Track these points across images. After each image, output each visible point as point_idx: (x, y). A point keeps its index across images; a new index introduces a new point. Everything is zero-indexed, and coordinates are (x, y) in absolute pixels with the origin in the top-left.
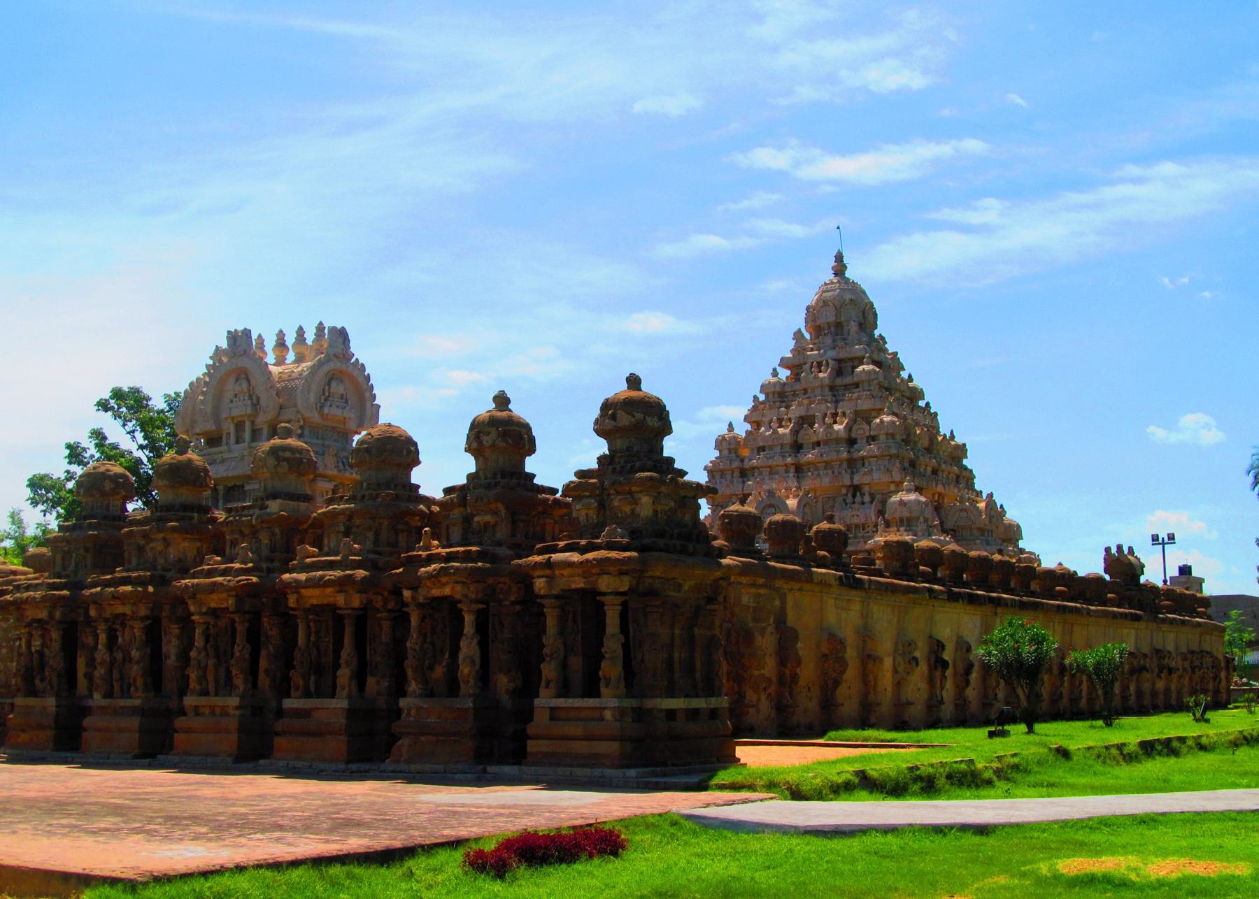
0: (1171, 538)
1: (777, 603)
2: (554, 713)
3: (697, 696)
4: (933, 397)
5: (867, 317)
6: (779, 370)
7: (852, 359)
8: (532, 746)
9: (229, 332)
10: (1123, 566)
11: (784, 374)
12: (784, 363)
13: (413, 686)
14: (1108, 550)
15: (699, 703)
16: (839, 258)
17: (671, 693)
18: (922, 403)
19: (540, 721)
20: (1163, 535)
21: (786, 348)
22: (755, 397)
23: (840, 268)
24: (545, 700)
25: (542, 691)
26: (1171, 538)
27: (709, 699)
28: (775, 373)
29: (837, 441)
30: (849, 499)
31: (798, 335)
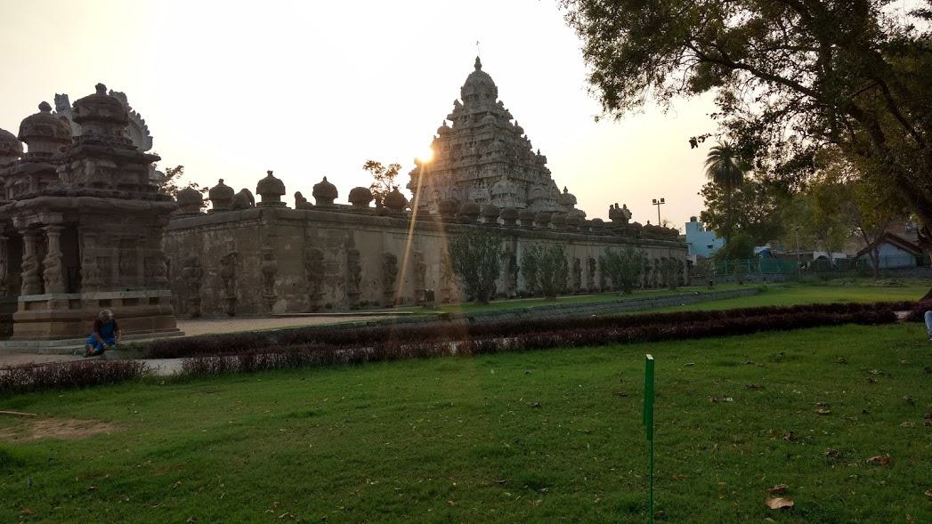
0: (663, 200)
1: (347, 236)
2: (28, 305)
3: (140, 290)
4: (530, 133)
7: (482, 113)
8: (17, 327)
9: (56, 95)
10: (620, 214)
12: (449, 118)
14: (612, 206)
15: (142, 294)
16: (478, 60)
17: (108, 286)
18: (523, 136)
19: (20, 313)
20: (658, 200)
21: (450, 109)
22: (435, 137)
23: (478, 65)
24: (24, 298)
25: (23, 292)
26: (663, 200)
27: (148, 292)
28: (444, 123)
29: (472, 156)
30: (477, 185)
31: (456, 103)
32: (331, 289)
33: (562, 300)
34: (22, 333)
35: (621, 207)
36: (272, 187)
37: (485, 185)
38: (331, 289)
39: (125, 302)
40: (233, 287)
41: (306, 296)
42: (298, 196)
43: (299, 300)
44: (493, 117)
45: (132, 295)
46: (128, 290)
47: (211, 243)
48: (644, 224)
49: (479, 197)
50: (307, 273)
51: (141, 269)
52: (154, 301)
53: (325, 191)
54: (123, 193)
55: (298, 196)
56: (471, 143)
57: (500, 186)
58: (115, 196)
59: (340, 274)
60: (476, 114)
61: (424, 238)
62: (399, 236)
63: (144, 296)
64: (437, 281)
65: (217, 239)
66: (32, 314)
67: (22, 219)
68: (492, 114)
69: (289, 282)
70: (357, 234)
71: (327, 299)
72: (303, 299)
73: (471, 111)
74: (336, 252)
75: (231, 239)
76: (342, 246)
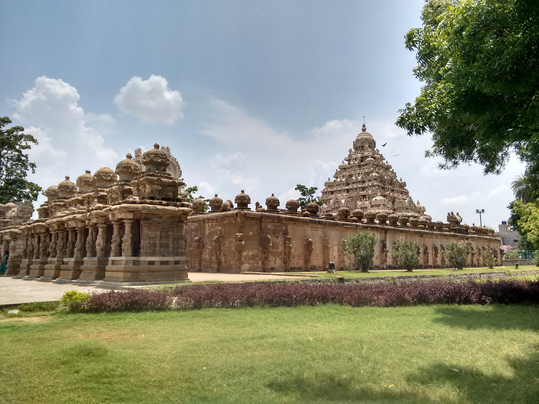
0: (483, 211)
2: (113, 262)
3: (169, 256)
5: (372, 144)
6: (345, 161)
7: (365, 157)
8: (107, 274)
11: (346, 163)
13: (88, 254)
14: (449, 214)
15: (170, 259)
16: (364, 126)
17: (153, 254)
20: (480, 210)
24: (112, 258)
25: (111, 255)
26: (483, 211)
27: (174, 257)
29: (359, 182)
32: (274, 259)
33: (416, 272)
34: (110, 277)
35: (455, 214)
36: (243, 201)
37: (367, 199)
38: (274, 259)
39: (162, 263)
40: (220, 254)
41: (260, 262)
42: (257, 204)
43: (256, 265)
44: (372, 159)
45: (166, 259)
46: (164, 256)
47: (209, 230)
48: (471, 225)
49: (363, 206)
50: (260, 248)
51: (171, 245)
52: (177, 263)
53: (273, 204)
54: (164, 202)
55: (257, 204)
56: (359, 174)
57: (376, 200)
58: (160, 204)
59: (279, 250)
60: (362, 158)
61: (329, 230)
62: (315, 229)
63: (172, 260)
64: (336, 257)
65: (213, 227)
66: (114, 267)
67: (113, 215)
68: (372, 157)
69: (250, 253)
70: (290, 227)
71: (271, 264)
72: (258, 264)
73: (359, 155)
74: (277, 237)
75: (220, 228)
76: (281, 234)
